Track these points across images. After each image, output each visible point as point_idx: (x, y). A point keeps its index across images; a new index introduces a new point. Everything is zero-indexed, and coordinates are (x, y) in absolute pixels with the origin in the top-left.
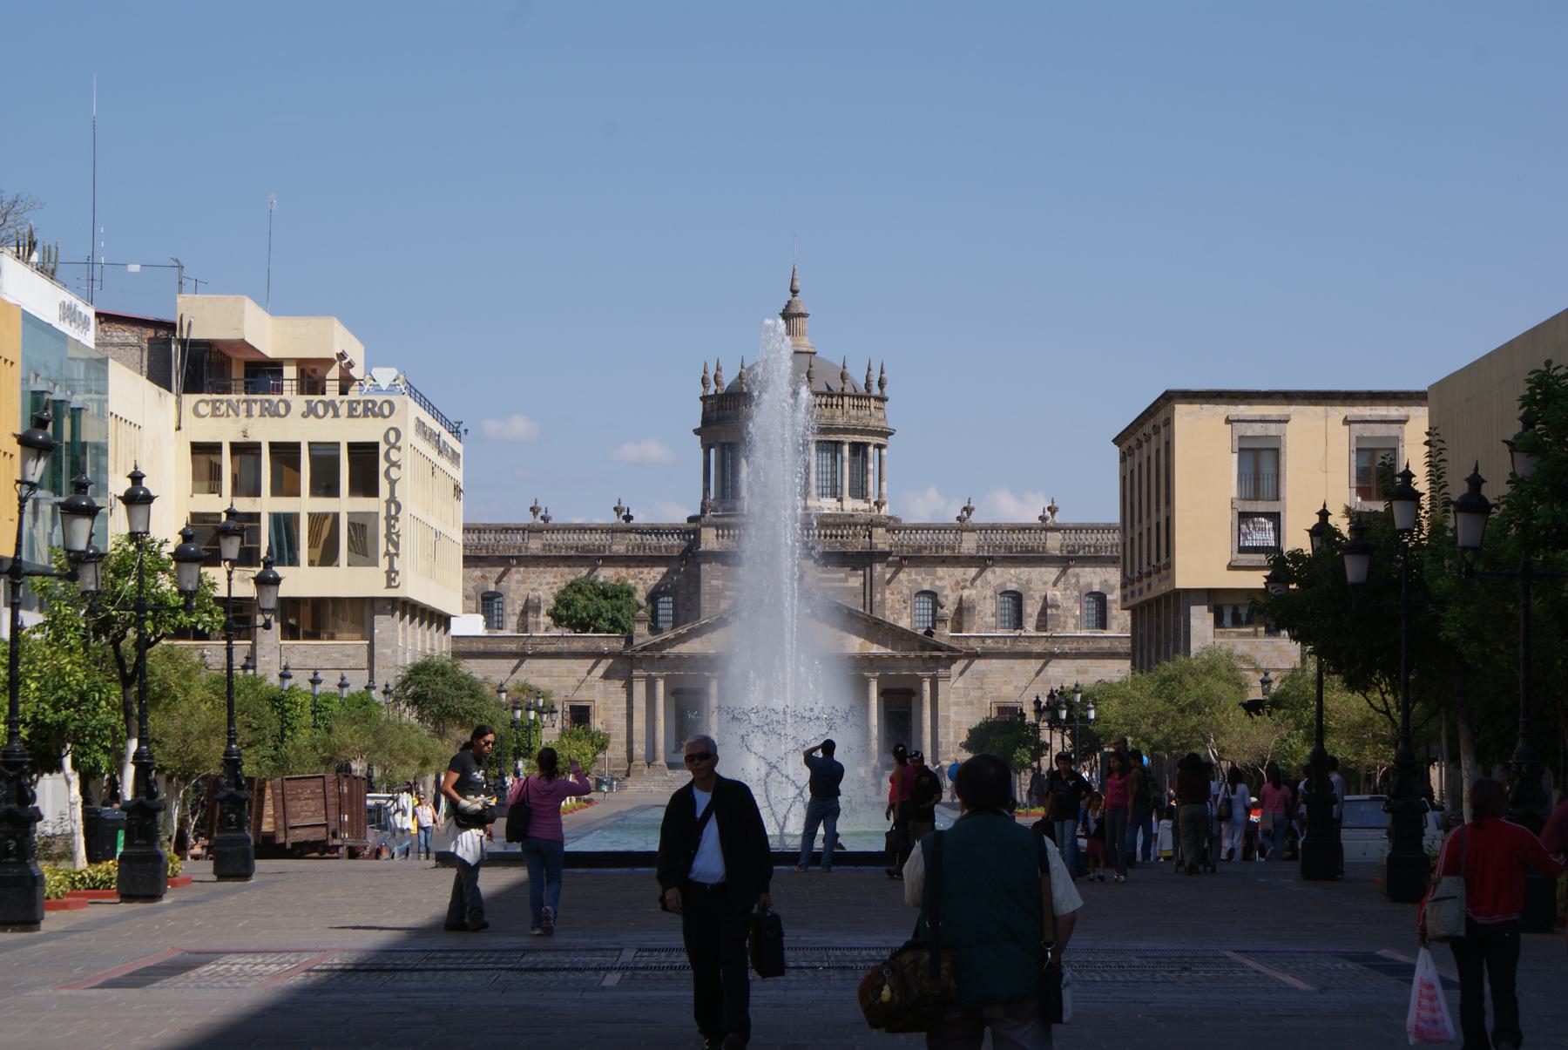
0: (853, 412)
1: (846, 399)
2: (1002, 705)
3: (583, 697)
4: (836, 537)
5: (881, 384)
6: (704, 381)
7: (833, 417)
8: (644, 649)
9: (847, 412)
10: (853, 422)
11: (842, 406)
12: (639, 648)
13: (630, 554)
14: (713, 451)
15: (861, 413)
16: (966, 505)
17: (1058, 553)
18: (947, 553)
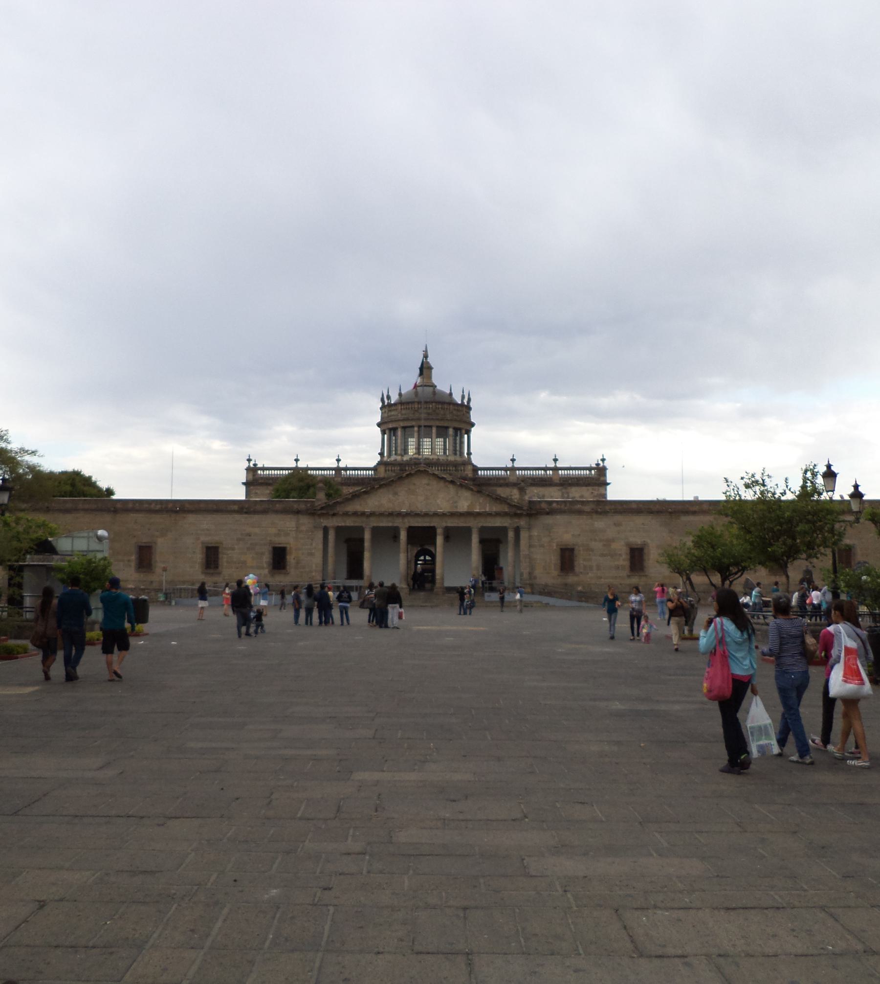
0: (455, 412)
1: (451, 406)
2: (564, 547)
3: (281, 541)
4: (447, 470)
5: (469, 400)
6: (382, 400)
7: (445, 414)
8: (322, 508)
9: (452, 412)
10: (455, 417)
11: (449, 409)
12: (319, 508)
13: (343, 482)
14: (386, 436)
15: (459, 413)
16: (512, 458)
17: (558, 482)
18: (502, 481)
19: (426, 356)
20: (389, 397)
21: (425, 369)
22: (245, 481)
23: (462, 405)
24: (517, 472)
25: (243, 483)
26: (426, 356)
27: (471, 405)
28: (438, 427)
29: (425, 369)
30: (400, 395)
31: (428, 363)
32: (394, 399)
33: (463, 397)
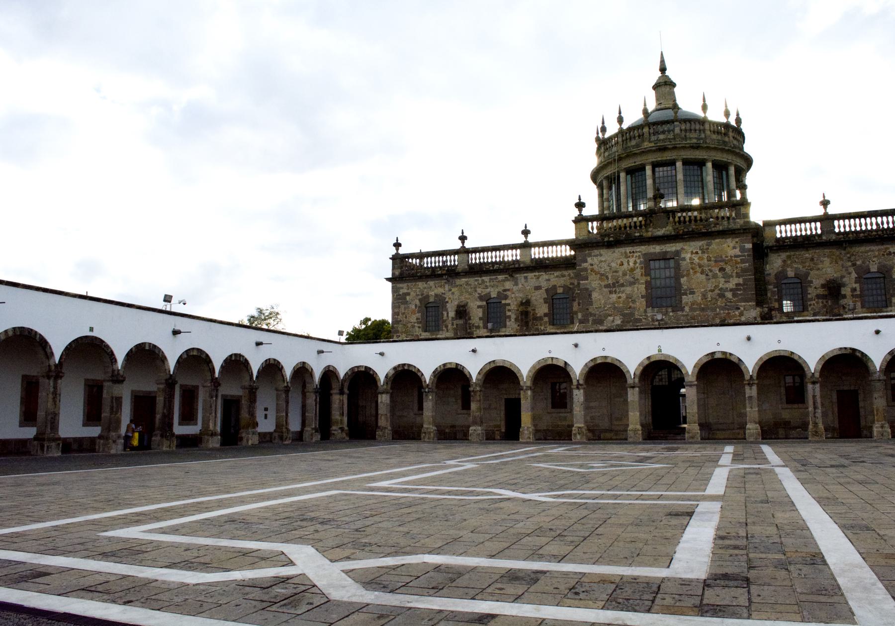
5: (738, 121)
19: (663, 69)
20: (604, 129)
21: (664, 86)
22: (390, 276)
23: (727, 126)
24: (836, 222)
25: (388, 279)
26: (663, 69)
27: (744, 127)
28: (686, 162)
29: (664, 86)
30: (620, 120)
31: (667, 77)
32: (612, 129)
33: (727, 114)
